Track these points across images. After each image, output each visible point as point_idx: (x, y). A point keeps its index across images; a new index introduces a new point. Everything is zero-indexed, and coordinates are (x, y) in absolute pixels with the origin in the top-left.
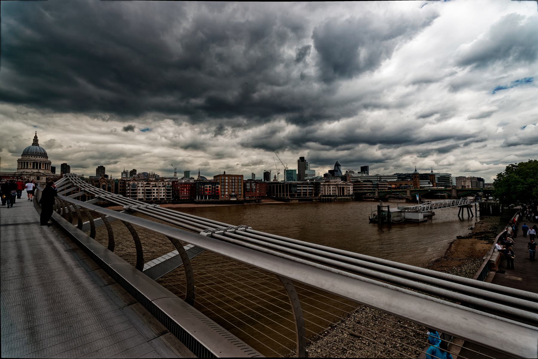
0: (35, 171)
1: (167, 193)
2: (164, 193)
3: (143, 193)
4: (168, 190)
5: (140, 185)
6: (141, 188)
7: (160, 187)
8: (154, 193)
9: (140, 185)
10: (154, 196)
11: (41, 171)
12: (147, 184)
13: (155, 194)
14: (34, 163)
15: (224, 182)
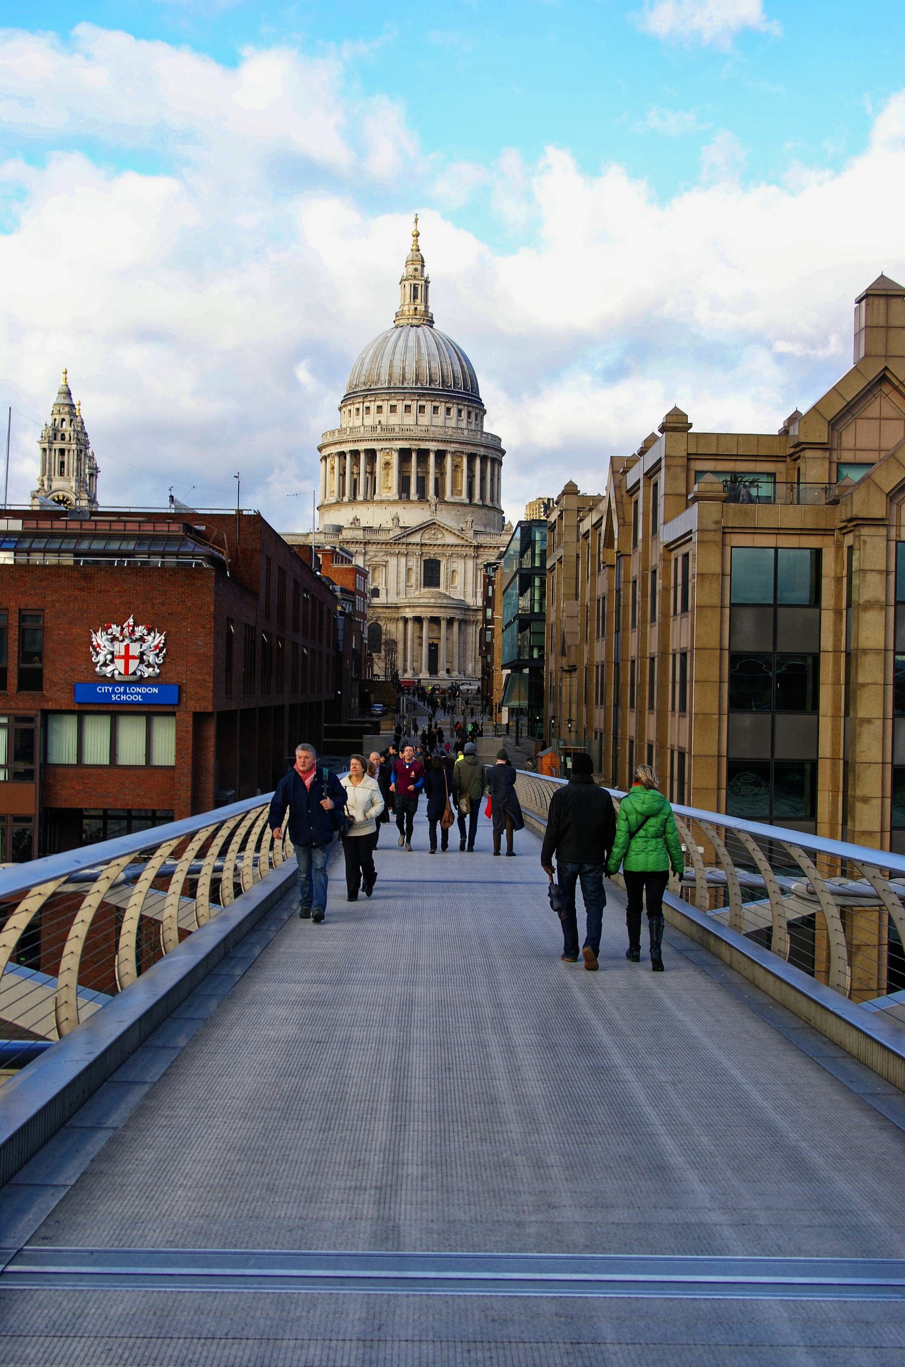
0: (413, 515)
14: (404, 454)
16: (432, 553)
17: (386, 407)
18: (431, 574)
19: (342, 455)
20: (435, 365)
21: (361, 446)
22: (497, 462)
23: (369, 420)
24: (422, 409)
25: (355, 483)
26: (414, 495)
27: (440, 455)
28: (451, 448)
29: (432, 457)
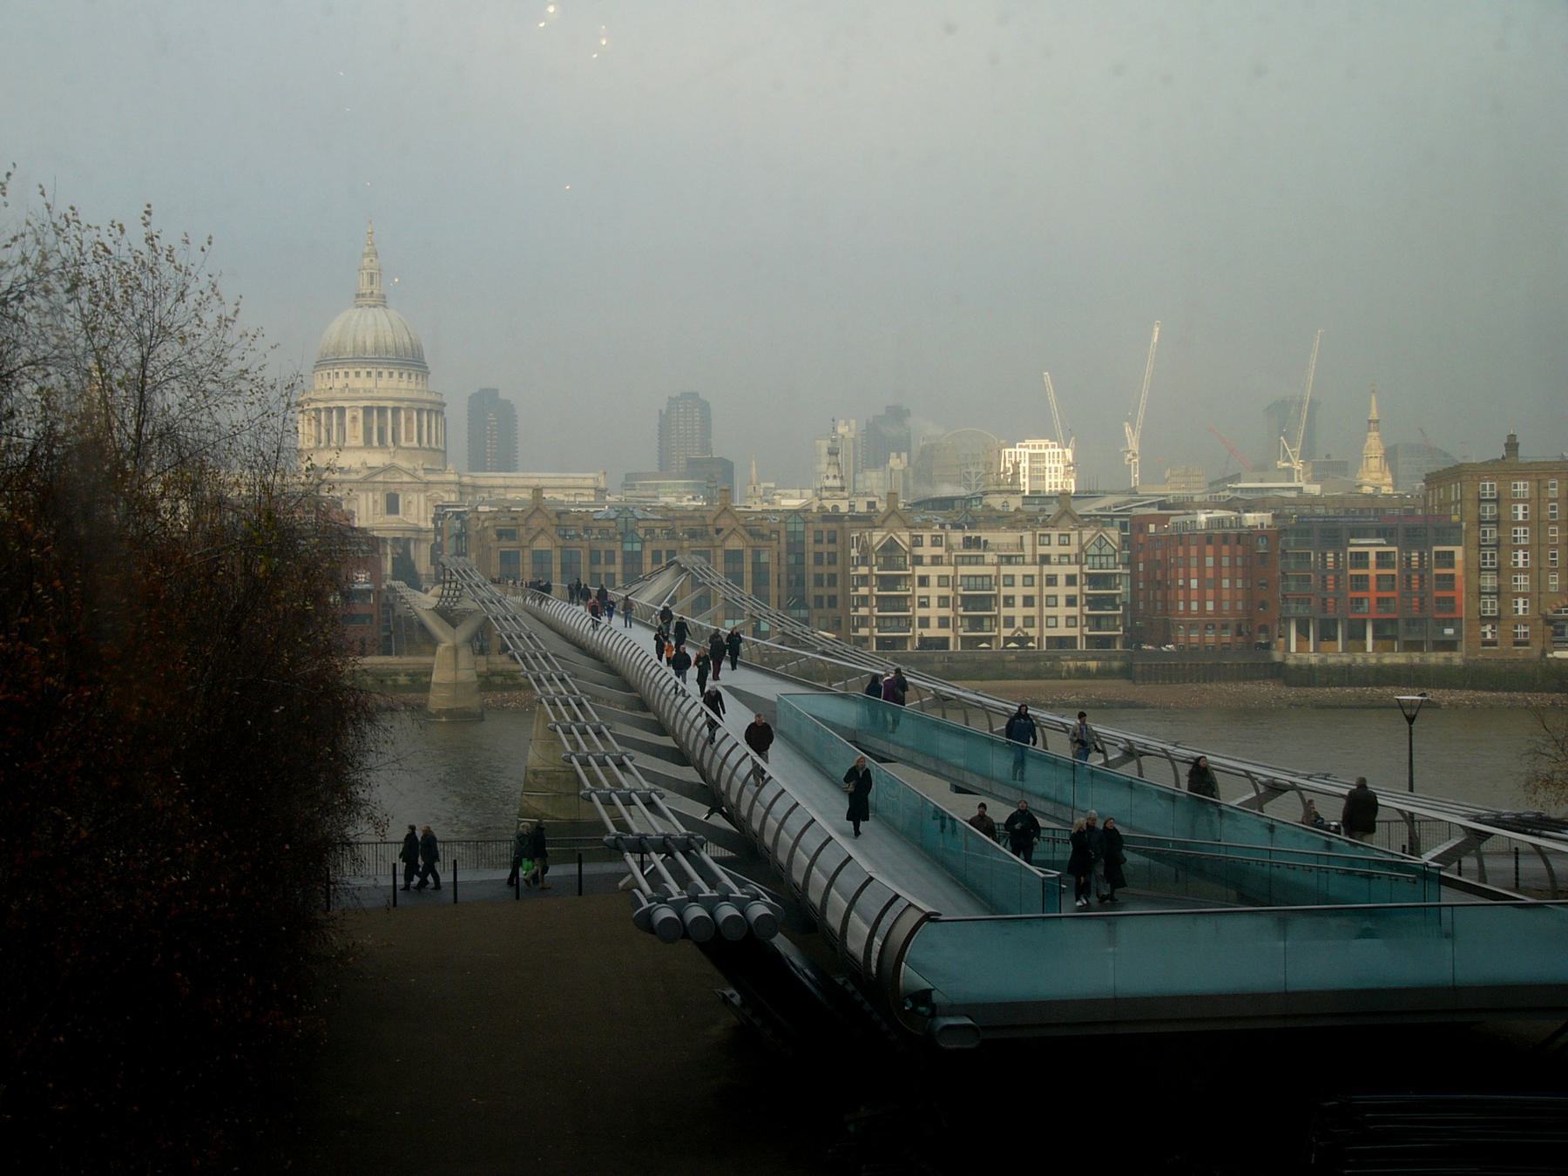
0: (377, 459)
1: (1094, 602)
2: (1071, 601)
3: (944, 601)
4: (1094, 580)
5: (927, 551)
6: (933, 572)
7: (1045, 559)
8: (1009, 601)
9: (927, 551)
10: (1010, 622)
11: (404, 464)
12: (969, 543)
13: (1019, 612)
14: (367, 411)
15: (1497, 521)
16: (392, 488)
17: (352, 374)
18: (392, 505)
19: (318, 410)
20: (389, 339)
21: (332, 405)
22: (439, 413)
23: (338, 384)
24: (380, 374)
25: (328, 432)
26: (376, 443)
27: (396, 410)
28: (404, 405)
29: (389, 413)
